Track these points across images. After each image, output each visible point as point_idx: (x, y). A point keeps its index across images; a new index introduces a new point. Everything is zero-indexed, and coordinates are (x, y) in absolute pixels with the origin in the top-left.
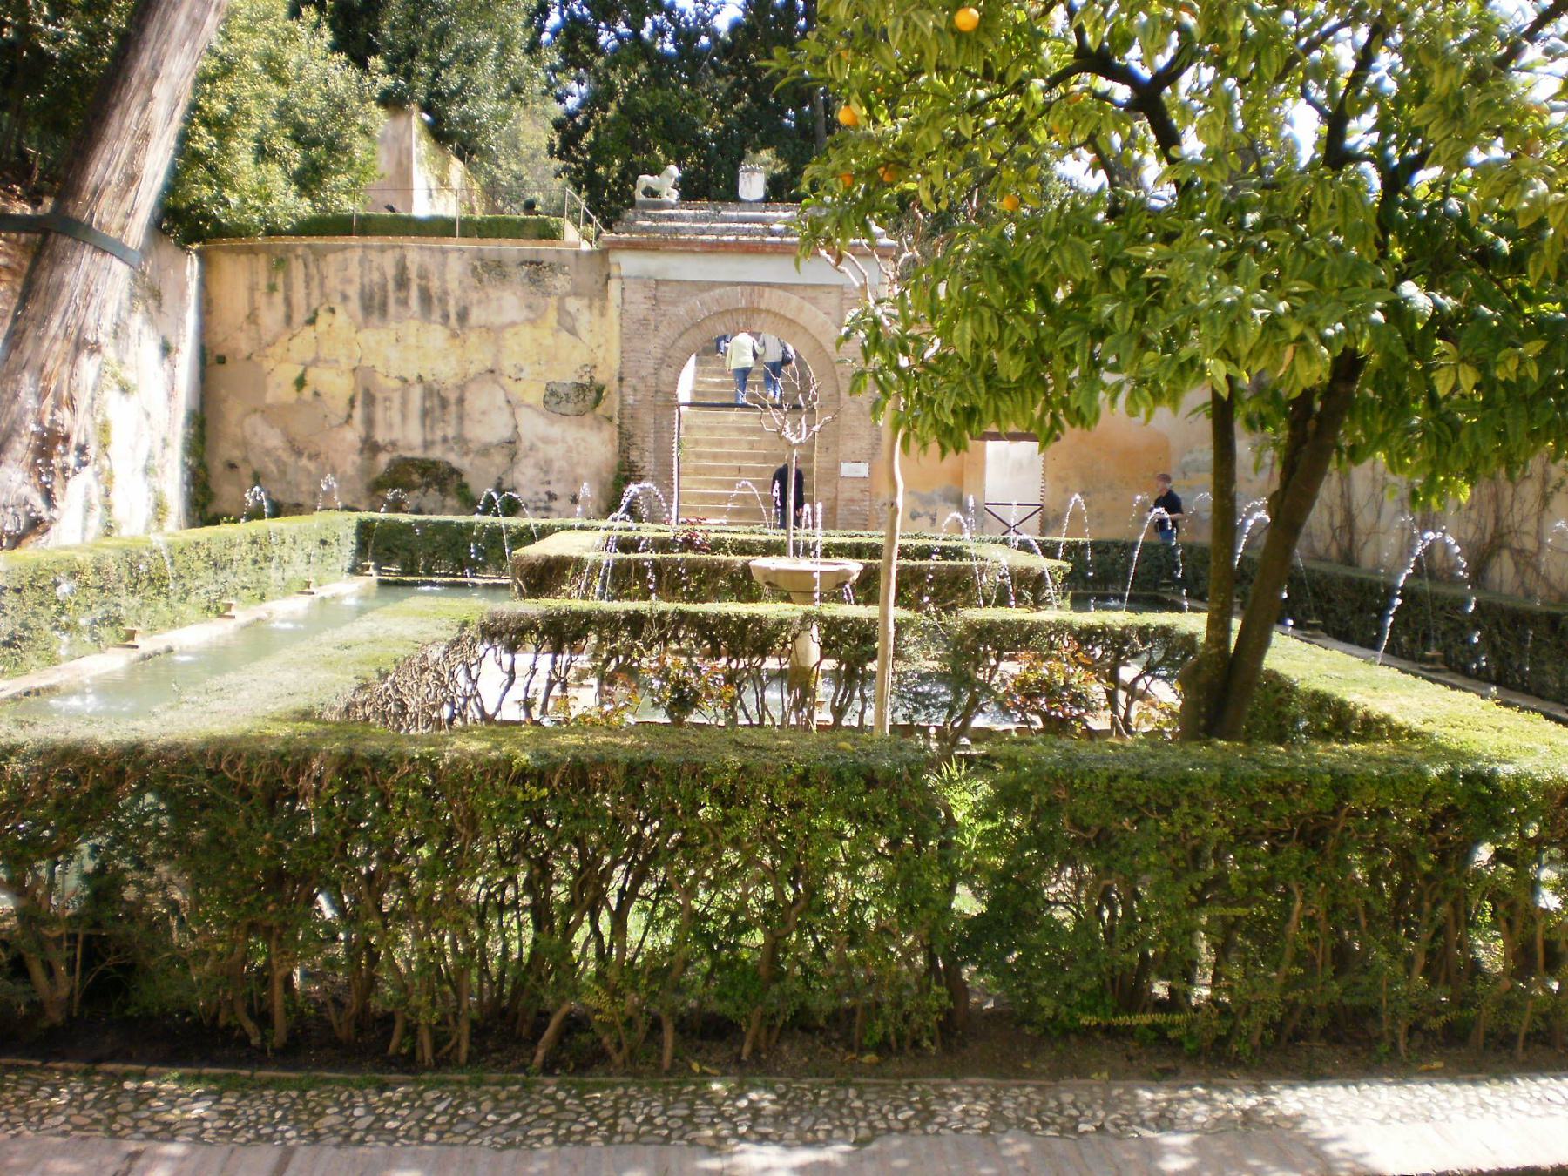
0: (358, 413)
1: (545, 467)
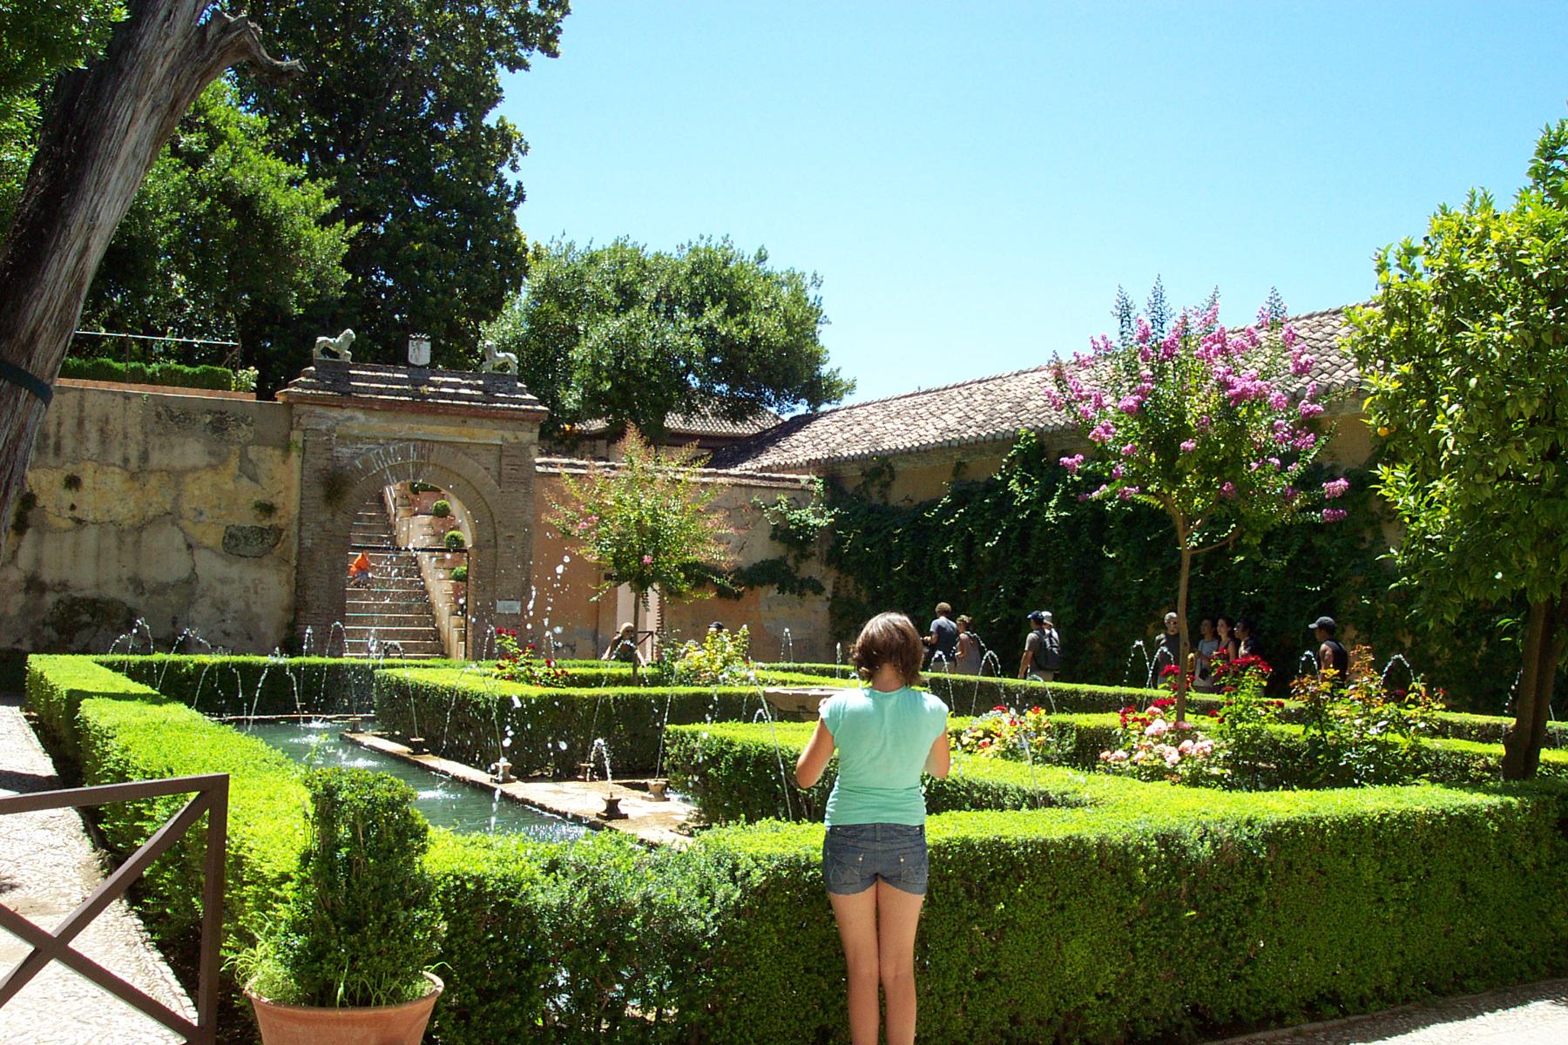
1: (221, 606)
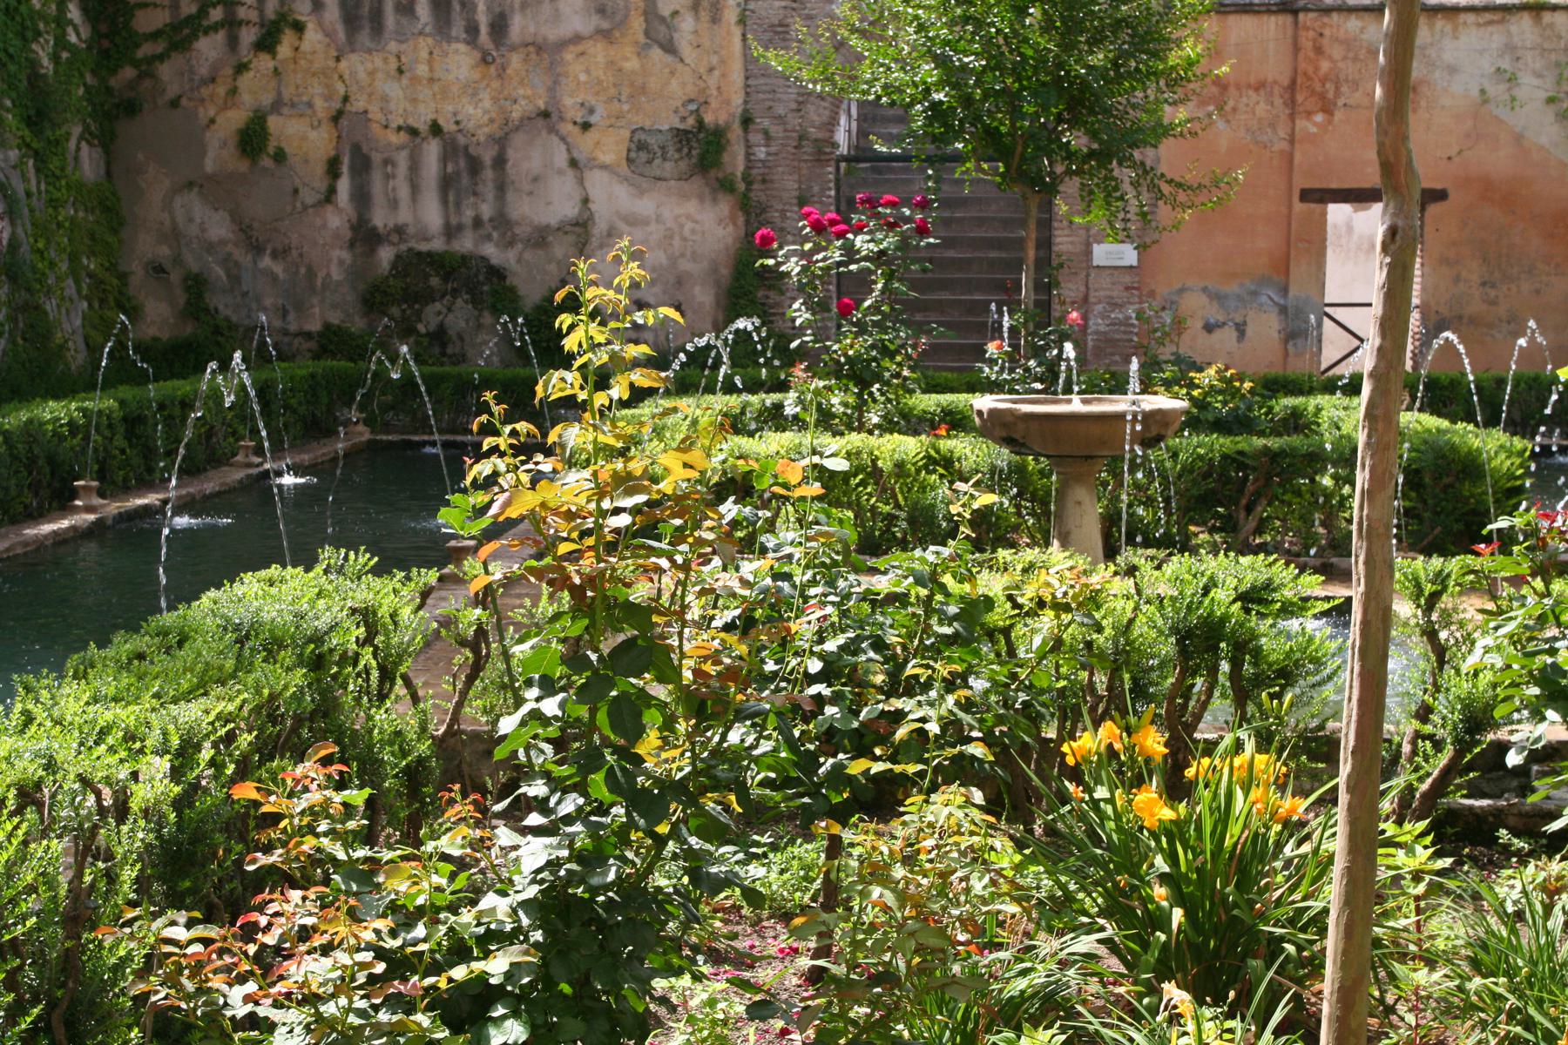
0: (344, 186)
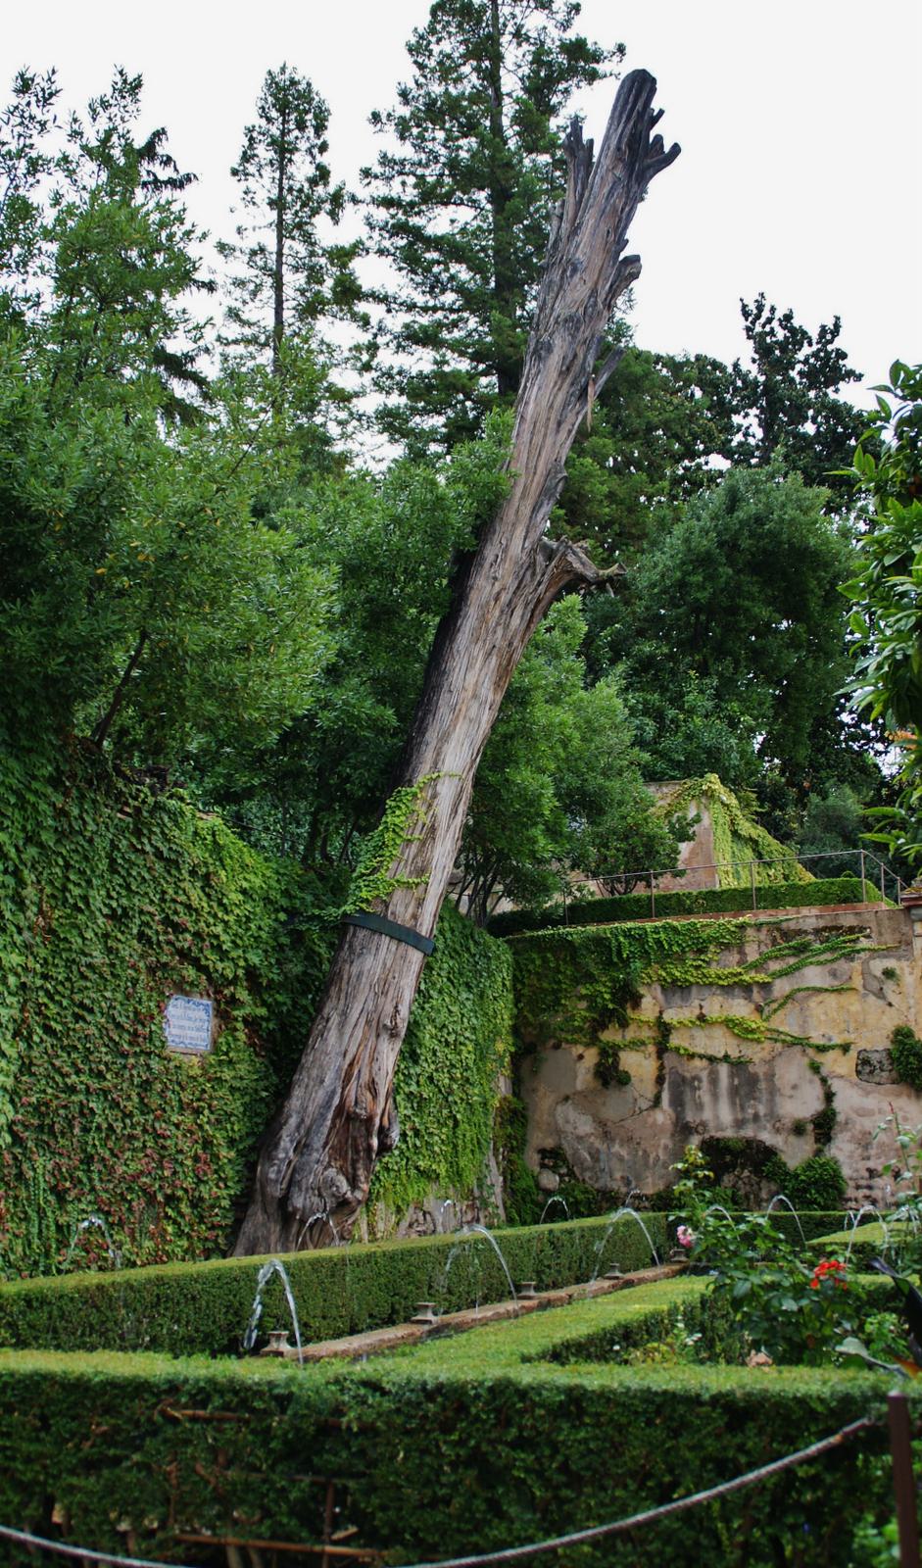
1: (865, 1142)
